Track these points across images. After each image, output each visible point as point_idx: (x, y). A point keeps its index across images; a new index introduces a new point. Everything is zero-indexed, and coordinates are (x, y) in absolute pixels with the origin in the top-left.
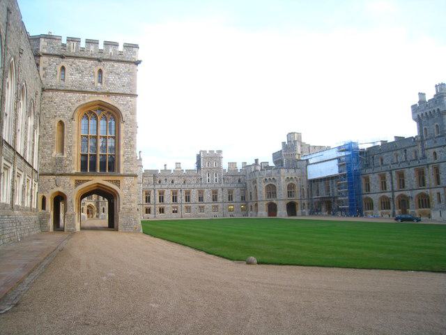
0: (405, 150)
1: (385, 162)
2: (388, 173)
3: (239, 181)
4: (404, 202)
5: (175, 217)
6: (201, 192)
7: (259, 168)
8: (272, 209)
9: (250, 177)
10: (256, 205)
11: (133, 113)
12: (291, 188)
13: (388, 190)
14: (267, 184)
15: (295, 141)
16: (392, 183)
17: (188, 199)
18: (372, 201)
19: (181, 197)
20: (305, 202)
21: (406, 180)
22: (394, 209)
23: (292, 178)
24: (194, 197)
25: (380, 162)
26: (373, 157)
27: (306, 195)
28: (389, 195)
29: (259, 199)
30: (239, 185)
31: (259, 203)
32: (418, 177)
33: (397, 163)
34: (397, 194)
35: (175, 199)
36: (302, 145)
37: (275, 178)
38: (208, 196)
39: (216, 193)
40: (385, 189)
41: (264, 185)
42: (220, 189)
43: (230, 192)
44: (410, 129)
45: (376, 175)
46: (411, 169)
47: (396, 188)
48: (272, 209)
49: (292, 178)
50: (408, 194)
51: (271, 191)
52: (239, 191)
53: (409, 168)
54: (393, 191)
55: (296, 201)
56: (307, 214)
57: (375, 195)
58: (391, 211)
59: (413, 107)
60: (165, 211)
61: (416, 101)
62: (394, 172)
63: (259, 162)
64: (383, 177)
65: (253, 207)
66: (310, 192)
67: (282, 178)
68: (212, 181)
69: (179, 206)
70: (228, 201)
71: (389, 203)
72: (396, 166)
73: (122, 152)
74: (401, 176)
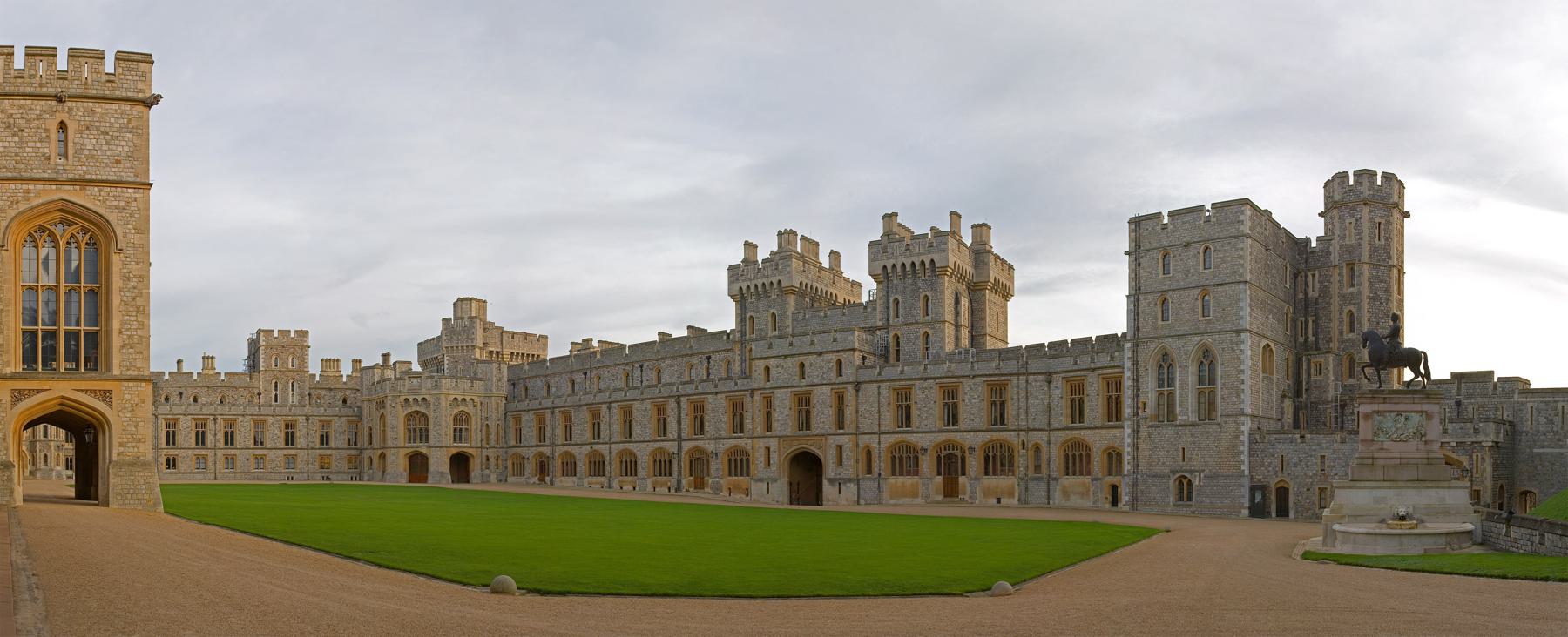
0: (709, 358)
1: (665, 378)
2: (673, 400)
4: (699, 464)
5: (199, 479)
6: (259, 424)
7: (389, 374)
8: (418, 466)
9: (370, 395)
10: (383, 456)
11: (143, 228)
12: (461, 420)
13: (670, 436)
14: (409, 410)
15: (471, 318)
16: (679, 423)
17: (229, 438)
18: (635, 456)
19: (214, 434)
20: (492, 454)
21: (706, 417)
22: (680, 474)
23: (464, 399)
24: (244, 435)
25: (655, 374)
26: (641, 366)
27: (493, 437)
28: (671, 447)
29: (390, 443)
31: (389, 453)
32: (730, 412)
33: (691, 382)
34: (687, 446)
35: (200, 438)
36: (488, 327)
38: (275, 434)
39: (293, 426)
40: (665, 434)
41: (402, 413)
43: (325, 423)
44: (724, 319)
45: (648, 405)
46: (719, 396)
47: (687, 429)
48: (418, 466)
49: (464, 399)
50: (709, 446)
51: (419, 427)
53: (717, 393)
54: (680, 439)
55: (470, 451)
56: (493, 478)
57: (643, 445)
58: (672, 482)
59: (732, 269)
60: (179, 463)
61: (738, 257)
62: (684, 400)
63: (392, 360)
64: (662, 410)
67: (443, 397)
69: (210, 453)
71: (670, 462)
72: (690, 389)
73: (116, 325)
74: (699, 409)
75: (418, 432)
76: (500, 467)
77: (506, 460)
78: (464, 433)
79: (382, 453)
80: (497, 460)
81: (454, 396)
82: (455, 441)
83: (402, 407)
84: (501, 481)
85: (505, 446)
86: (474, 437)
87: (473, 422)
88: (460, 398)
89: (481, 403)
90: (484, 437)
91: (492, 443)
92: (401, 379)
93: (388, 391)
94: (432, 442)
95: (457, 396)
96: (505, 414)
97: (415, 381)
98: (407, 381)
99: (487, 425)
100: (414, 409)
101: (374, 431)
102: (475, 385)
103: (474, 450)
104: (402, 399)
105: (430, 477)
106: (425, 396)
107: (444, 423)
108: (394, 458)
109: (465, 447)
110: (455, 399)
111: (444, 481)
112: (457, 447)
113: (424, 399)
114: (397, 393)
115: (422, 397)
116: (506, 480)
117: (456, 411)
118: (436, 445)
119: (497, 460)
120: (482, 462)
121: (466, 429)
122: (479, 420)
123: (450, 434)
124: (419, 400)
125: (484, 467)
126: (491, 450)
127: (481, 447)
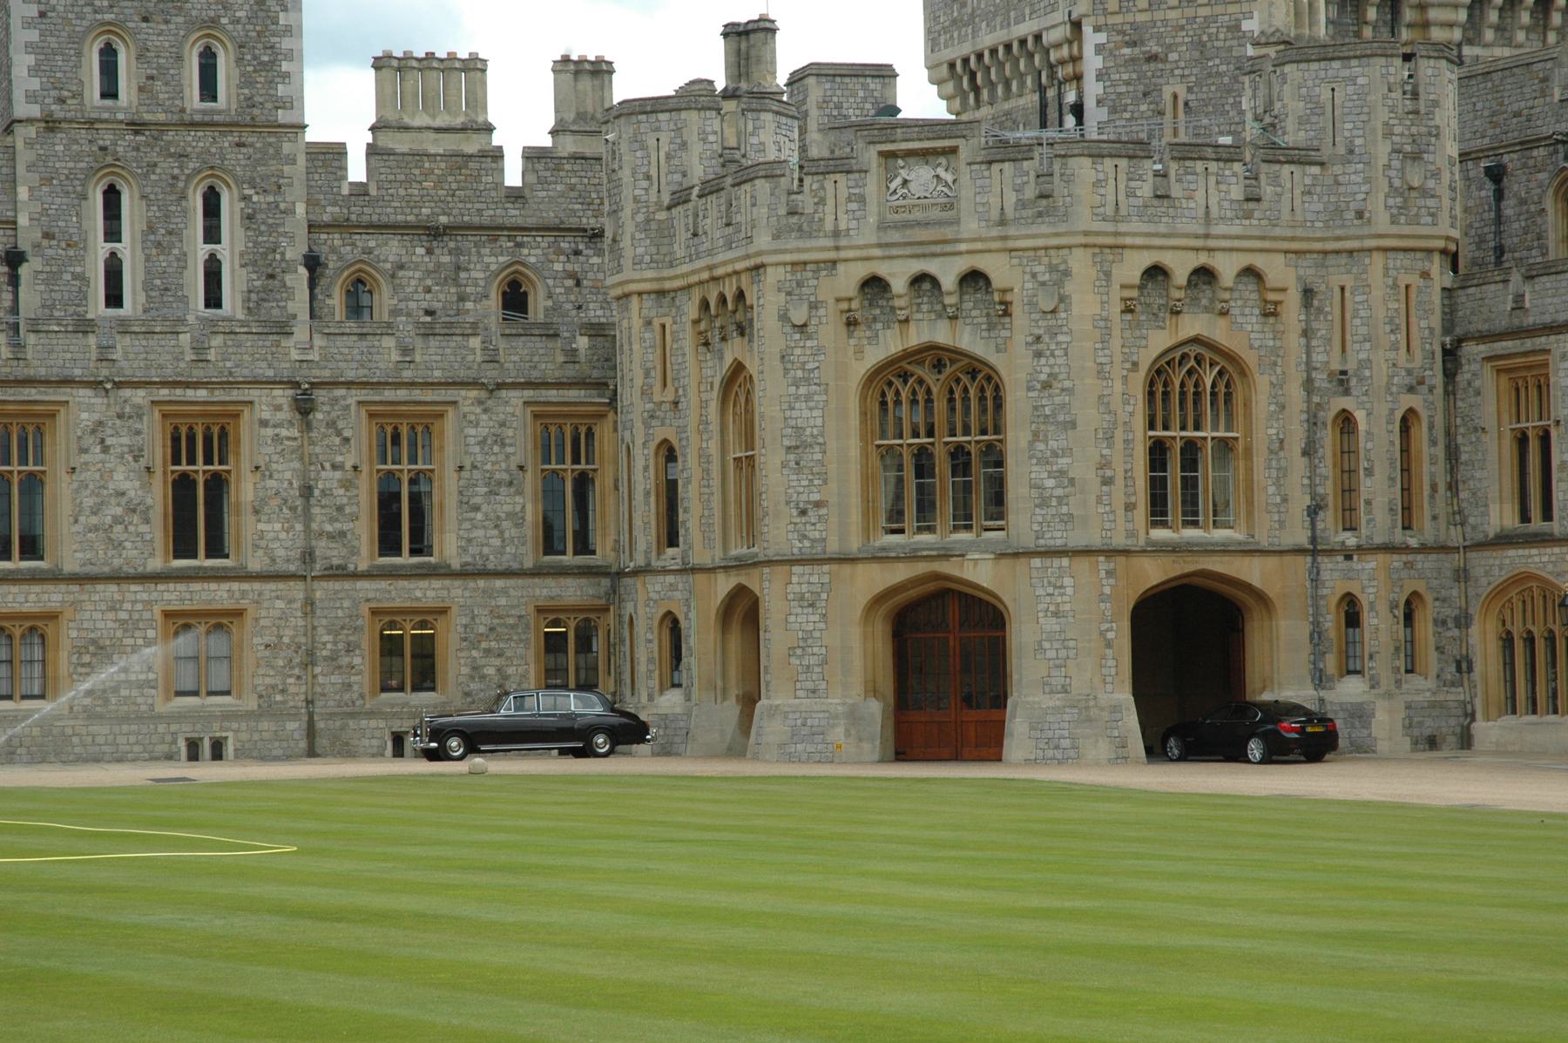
3: (515, 299)
14: (890, 344)
23: (1204, 275)
29: (779, 535)
30: (519, 355)
31: (772, 591)
37: (999, 270)
42: (272, 405)
49: (1204, 275)
52: (521, 442)
55: (1251, 571)
56: (1386, 722)
65: (701, 637)
66: (1431, 463)
67: (1080, 262)
68: (163, 289)
70: (365, 554)
75: (942, 465)
76: (1430, 659)
77: (1463, 621)
78: (1208, 471)
79: (740, 592)
80: (1409, 618)
81: (1147, 259)
82: (1158, 509)
83: (851, 323)
84: (1432, 743)
85: (1455, 537)
86: (1267, 490)
87: (1262, 403)
88: (1181, 267)
89: (1308, 293)
90: (1328, 489)
91: (1378, 521)
92: (839, 165)
93: (763, 240)
94: (1023, 521)
95: (1167, 259)
96: (1451, 355)
97: (921, 176)
98: (872, 186)
99: (1346, 421)
100: (918, 336)
101: (689, 471)
102: (1268, 191)
103: (1272, 562)
104: (850, 277)
105: (1018, 727)
106: (983, 263)
107: (1088, 415)
108: (807, 620)
109: (1225, 550)
110: (1156, 273)
111: (1104, 749)
112: (1174, 549)
113: (974, 279)
114: (817, 248)
115: (962, 265)
116: (1466, 741)
117: (1159, 341)
118: (1056, 538)
119: (1409, 618)
120: (1317, 635)
121: (1225, 446)
122: (1296, 393)
123: (1128, 476)
124: (948, 281)
125: (1331, 663)
126: (1371, 563)
127: (1315, 550)
